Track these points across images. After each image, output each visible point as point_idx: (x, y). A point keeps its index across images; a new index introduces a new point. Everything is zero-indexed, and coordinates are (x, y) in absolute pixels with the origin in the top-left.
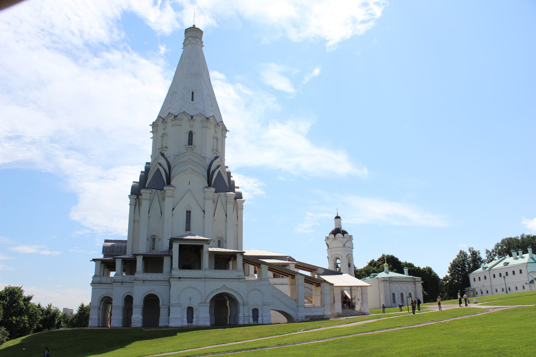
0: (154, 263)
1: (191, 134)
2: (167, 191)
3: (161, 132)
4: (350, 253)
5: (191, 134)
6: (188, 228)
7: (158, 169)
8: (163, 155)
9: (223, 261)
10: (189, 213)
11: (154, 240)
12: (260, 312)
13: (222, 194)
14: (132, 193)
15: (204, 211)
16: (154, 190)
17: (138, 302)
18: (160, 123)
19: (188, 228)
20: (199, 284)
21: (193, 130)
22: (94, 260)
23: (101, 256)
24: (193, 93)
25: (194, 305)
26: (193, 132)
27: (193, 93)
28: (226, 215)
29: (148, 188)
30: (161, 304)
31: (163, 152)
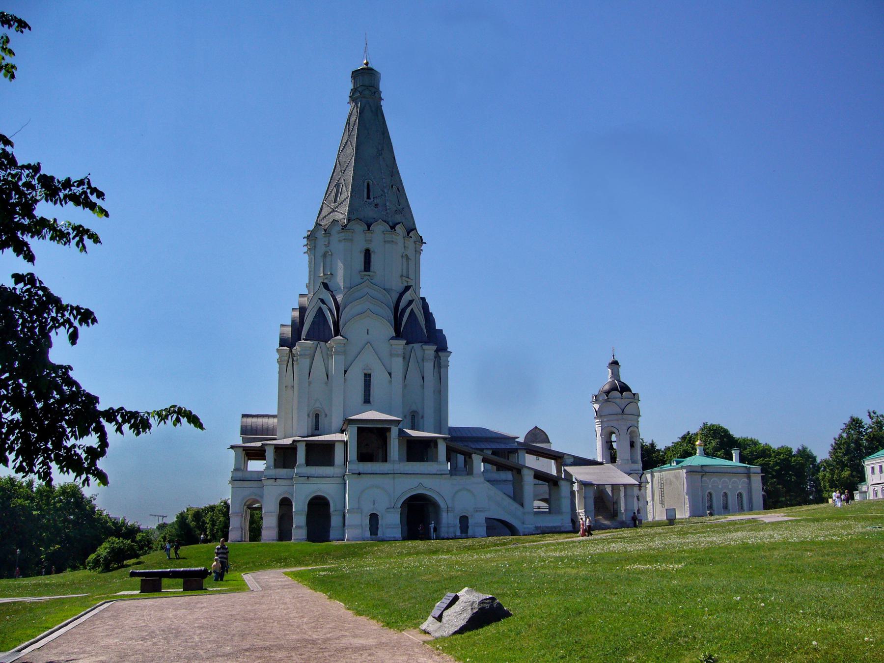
0: (320, 454)
1: (367, 254)
3: (321, 249)
4: (635, 423)
5: (367, 254)
6: (367, 400)
7: (320, 309)
8: (326, 286)
9: (419, 450)
10: (367, 377)
11: (317, 416)
12: (470, 521)
13: (416, 346)
14: (281, 345)
16: (316, 342)
17: (299, 508)
19: (367, 400)
20: (386, 481)
21: (372, 247)
22: (232, 447)
23: (239, 441)
25: (380, 510)
26: (372, 250)
30: (332, 509)
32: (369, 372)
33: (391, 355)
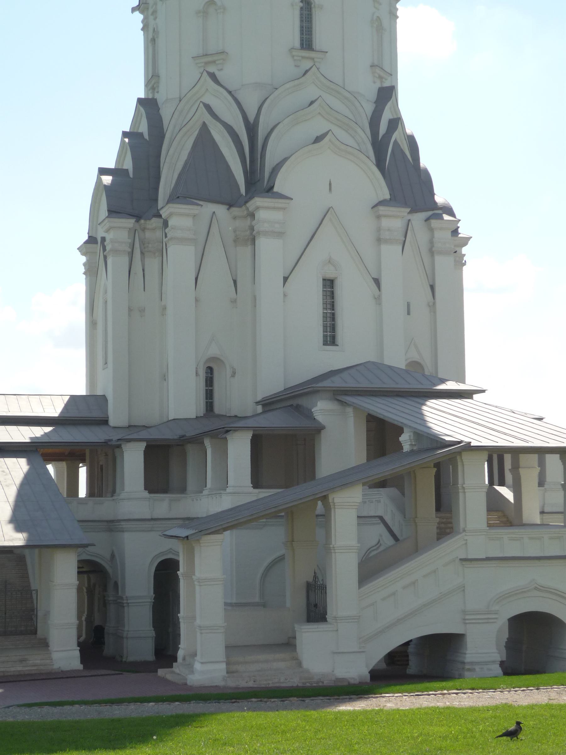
2: (262, 215)
6: (330, 338)
7: (204, 129)
8: (213, 76)
10: (329, 285)
15: (377, 282)
19: (330, 338)
28: (432, 288)
29: (176, 197)
31: (211, 69)
32: (330, 276)
33: (379, 241)
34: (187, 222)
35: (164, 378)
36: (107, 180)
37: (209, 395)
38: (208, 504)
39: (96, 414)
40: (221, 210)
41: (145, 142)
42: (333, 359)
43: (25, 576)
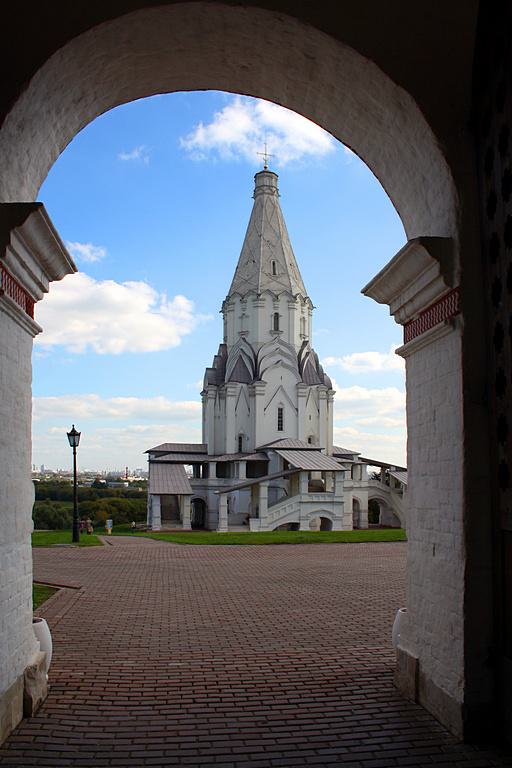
6: (280, 428)
8: (244, 339)
10: (281, 411)
15: (297, 410)
18: (237, 300)
19: (280, 428)
24: (274, 263)
27: (274, 263)
34: (233, 390)
35: (225, 439)
36: (209, 372)
37: (240, 446)
38: (234, 483)
39: (204, 451)
40: (244, 385)
41: (222, 359)
42: (281, 435)
43: (177, 503)
